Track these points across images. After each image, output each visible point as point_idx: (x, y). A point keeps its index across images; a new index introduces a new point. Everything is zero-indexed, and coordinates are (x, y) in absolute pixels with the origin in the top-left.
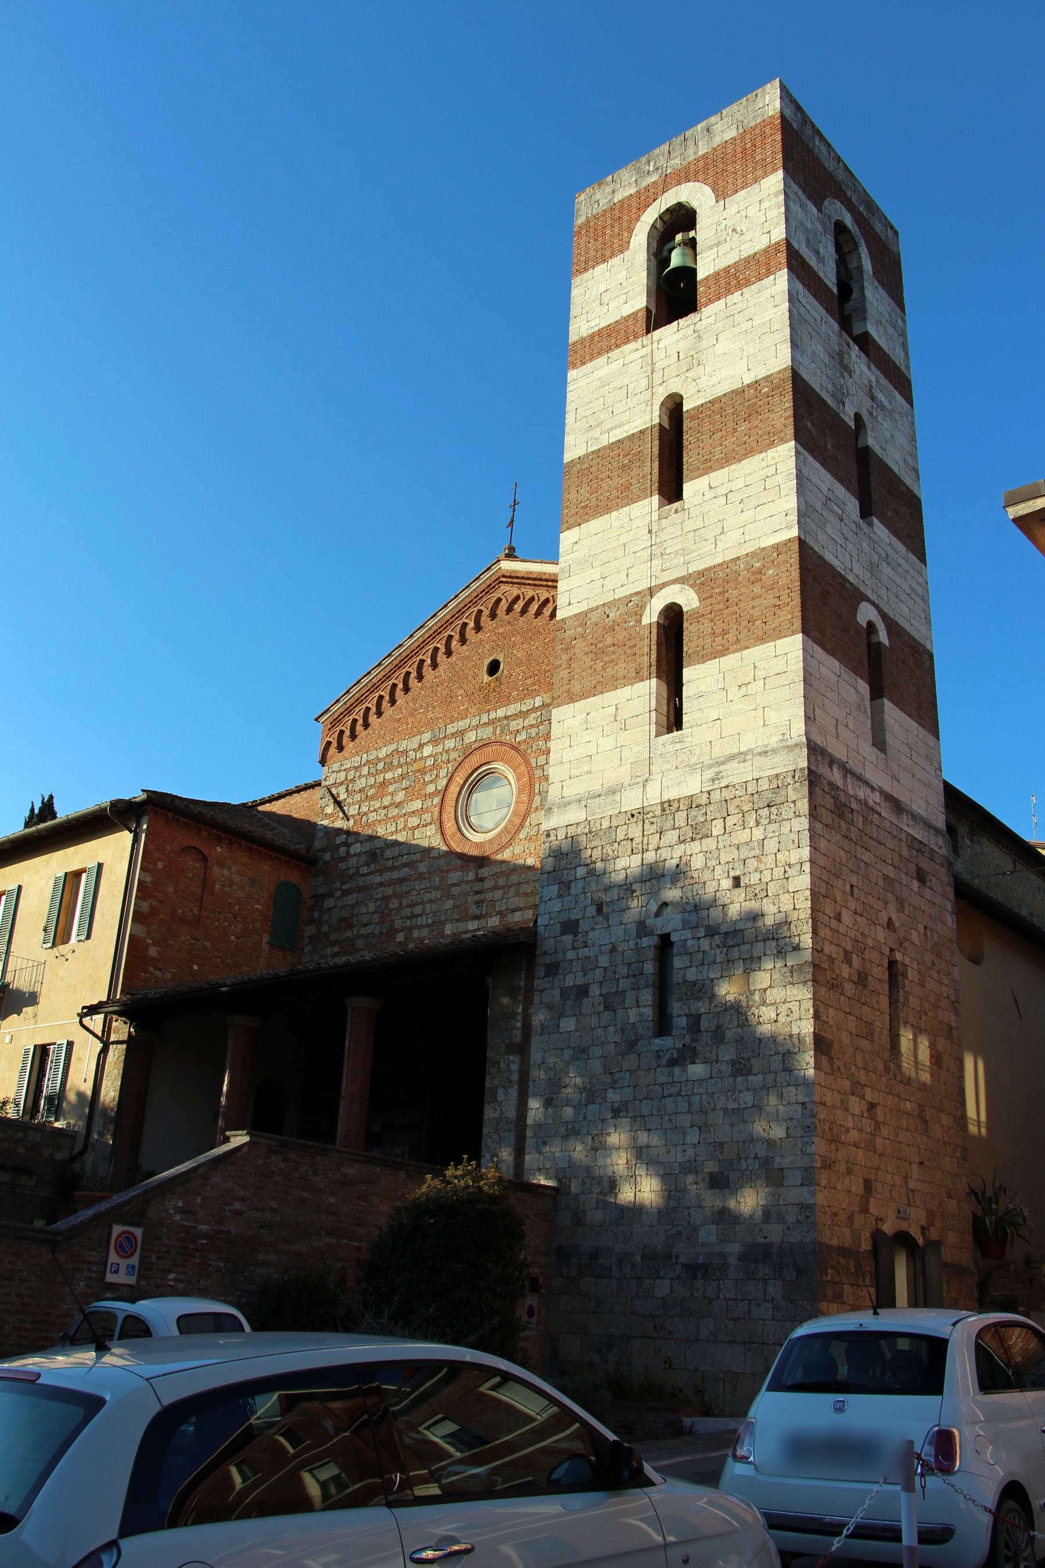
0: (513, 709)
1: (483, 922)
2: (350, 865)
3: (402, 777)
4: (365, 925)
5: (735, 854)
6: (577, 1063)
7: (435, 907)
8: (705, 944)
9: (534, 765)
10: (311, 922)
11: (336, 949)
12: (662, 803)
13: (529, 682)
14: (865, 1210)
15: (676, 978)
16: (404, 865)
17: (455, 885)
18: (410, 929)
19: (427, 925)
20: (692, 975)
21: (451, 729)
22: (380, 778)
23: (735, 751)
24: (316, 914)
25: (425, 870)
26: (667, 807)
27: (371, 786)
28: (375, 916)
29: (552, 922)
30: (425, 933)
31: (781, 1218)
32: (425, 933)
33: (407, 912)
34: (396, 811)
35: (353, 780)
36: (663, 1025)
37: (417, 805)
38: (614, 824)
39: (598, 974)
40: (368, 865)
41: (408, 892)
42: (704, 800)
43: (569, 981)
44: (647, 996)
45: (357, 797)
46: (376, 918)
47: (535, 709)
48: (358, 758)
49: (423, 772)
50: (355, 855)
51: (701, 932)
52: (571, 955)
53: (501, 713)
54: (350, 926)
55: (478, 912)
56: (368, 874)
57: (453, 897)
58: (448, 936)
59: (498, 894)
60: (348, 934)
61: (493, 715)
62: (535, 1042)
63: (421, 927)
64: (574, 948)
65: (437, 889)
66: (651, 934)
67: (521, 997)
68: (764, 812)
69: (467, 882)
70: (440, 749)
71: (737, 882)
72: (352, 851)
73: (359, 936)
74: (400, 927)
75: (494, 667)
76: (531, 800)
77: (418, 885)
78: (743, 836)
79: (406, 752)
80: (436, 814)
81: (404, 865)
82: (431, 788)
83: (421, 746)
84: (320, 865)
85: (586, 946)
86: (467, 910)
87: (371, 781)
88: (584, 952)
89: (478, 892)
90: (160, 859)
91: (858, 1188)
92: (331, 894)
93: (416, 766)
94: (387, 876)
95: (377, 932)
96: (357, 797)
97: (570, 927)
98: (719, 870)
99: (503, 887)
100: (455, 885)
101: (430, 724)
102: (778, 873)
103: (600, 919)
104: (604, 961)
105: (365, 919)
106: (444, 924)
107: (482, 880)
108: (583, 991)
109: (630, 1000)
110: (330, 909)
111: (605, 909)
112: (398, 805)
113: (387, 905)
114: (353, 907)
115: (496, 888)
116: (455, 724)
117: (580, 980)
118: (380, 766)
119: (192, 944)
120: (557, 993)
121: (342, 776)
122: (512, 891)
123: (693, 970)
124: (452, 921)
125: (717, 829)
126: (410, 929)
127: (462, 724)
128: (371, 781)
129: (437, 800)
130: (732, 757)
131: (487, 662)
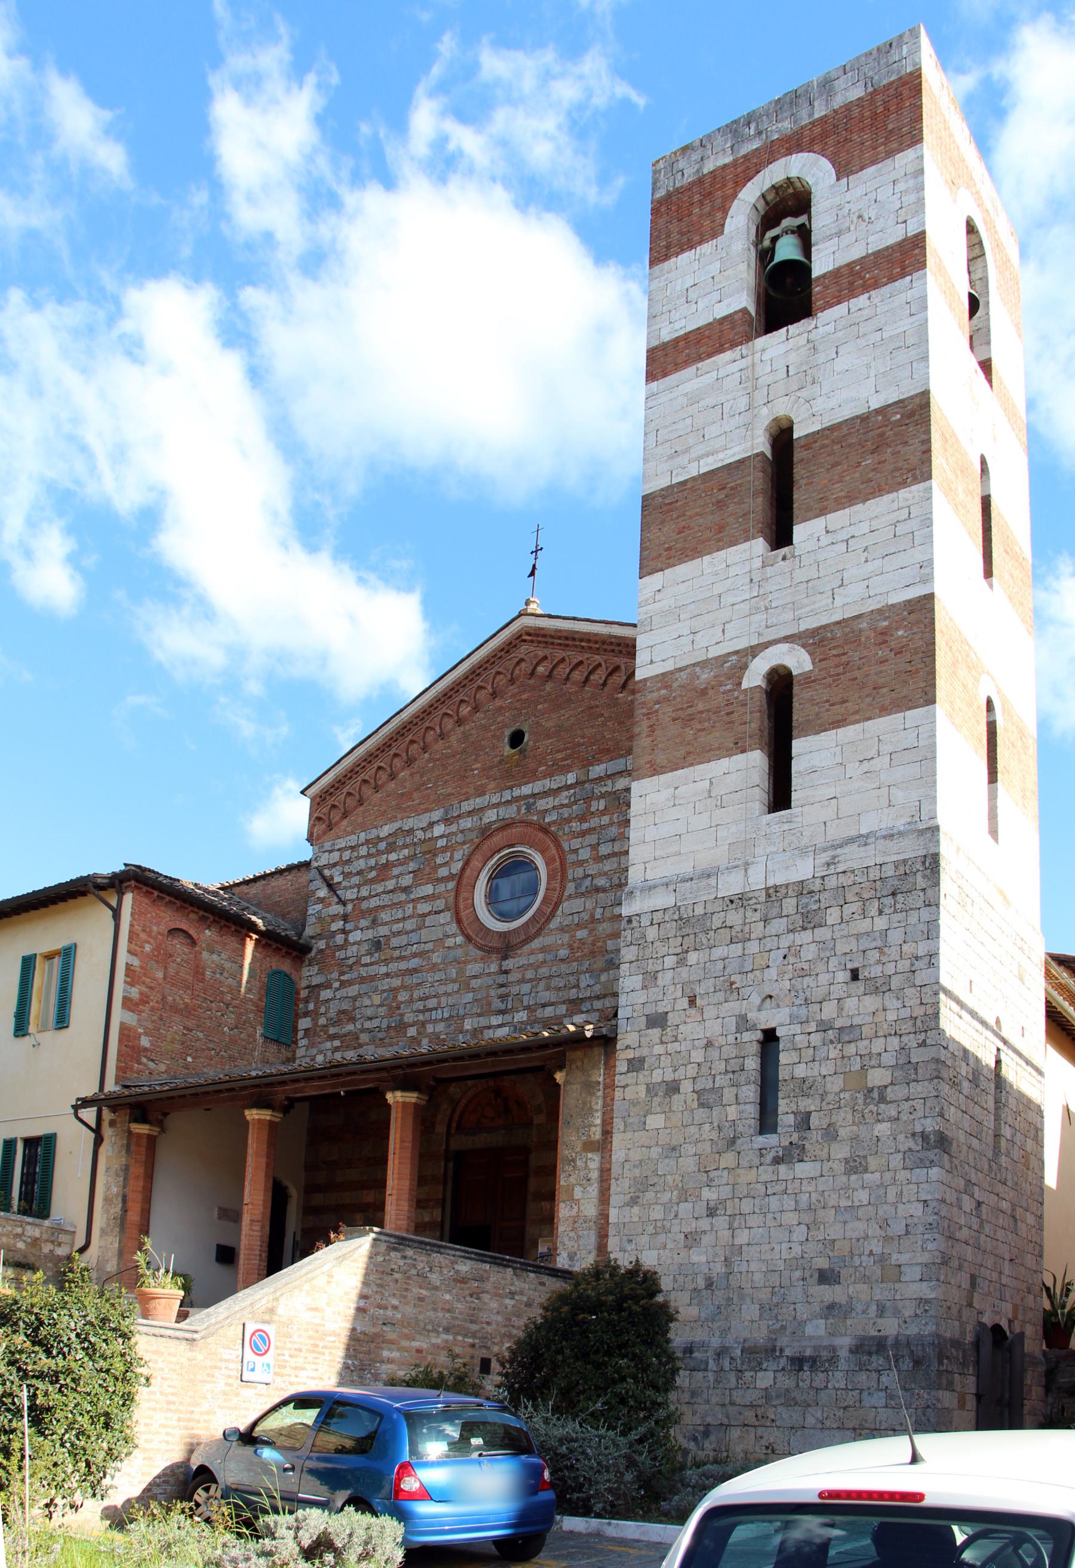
0: (538, 786)
1: (508, 1018)
4: (370, 1019)
6: (667, 1161)
8: (816, 1039)
9: (567, 849)
12: (767, 889)
13: (560, 756)
14: (970, 1305)
15: (783, 1074)
16: (415, 955)
17: (475, 977)
18: (423, 1024)
19: (442, 1020)
20: (800, 1071)
21: (466, 806)
22: (383, 859)
23: (853, 833)
24: (311, 1006)
25: (439, 961)
27: (372, 868)
28: (380, 1009)
29: (635, 1015)
30: (440, 1027)
31: (897, 1313)
32: (440, 1027)
33: (420, 1005)
34: (403, 897)
35: (349, 861)
36: (767, 1122)
37: (428, 889)
39: (692, 1070)
41: (419, 984)
43: (657, 1077)
44: (751, 1093)
45: (356, 880)
46: (382, 1011)
47: (568, 787)
48: (354, 837)
49: (434, 852)
50: (354, 943)
51: (812, 1027)
52: (659, 1049)
53: (526, 790)
54: (353, 1020)
55: (503, 1007)
56: (372, 964)
57: (474, 990)
58: (467, 1031)
59: (526, 988)
60: (350, 1027)
61: (517, 792)
63: (436, 1021)
64: (662, 1042)
65: (454, 981)
66: (753, 1028)
67: (600, 1093)
69: (489, 974)
70: (454, 828)
74: (411, 1021)
75: (516, 739)
76: (563, 888)
77: (430, 977)
79: (411, 831)
80: (451, 899)
81: (415, 955)
82: (443, 872)
83: (431, 825)
84: (313, 954)
85: (676, 1041)
86: (489, 1004)
87: (372, 862)
88: (673, 1047)
89: (502, 986)
90: (148, 942)
91: (966, 1284)
92: (327, 985)
93: (425, 847)
94: (393, 967)
95: (384, 1026)
96: (356, 880)
97: (657, 1021)
99: (530, 981)
100: (475, 977)
101: (441, 801)
103: (693, 1011)
104: (698, 1056)
105: (369, 1012)
106: (463, 1018)
107: (506, 972)
108: (673, 1088)
109: (728, 1095)
110: (328, 1001)
111: (698, 1002)
112: (406, 890)
114: (354, 999)
115: (523, 981)
116: (471, 802)
117: (669, 1076)
118: (382, 846)
119: (184, 1034)
120: (642, 1089)
121: (335, 856)
122: (542, 984)
123: (803, 1066)
126: (423, 1024)
127: (479, 802)
128: (372, 862)
129: (451, 885)
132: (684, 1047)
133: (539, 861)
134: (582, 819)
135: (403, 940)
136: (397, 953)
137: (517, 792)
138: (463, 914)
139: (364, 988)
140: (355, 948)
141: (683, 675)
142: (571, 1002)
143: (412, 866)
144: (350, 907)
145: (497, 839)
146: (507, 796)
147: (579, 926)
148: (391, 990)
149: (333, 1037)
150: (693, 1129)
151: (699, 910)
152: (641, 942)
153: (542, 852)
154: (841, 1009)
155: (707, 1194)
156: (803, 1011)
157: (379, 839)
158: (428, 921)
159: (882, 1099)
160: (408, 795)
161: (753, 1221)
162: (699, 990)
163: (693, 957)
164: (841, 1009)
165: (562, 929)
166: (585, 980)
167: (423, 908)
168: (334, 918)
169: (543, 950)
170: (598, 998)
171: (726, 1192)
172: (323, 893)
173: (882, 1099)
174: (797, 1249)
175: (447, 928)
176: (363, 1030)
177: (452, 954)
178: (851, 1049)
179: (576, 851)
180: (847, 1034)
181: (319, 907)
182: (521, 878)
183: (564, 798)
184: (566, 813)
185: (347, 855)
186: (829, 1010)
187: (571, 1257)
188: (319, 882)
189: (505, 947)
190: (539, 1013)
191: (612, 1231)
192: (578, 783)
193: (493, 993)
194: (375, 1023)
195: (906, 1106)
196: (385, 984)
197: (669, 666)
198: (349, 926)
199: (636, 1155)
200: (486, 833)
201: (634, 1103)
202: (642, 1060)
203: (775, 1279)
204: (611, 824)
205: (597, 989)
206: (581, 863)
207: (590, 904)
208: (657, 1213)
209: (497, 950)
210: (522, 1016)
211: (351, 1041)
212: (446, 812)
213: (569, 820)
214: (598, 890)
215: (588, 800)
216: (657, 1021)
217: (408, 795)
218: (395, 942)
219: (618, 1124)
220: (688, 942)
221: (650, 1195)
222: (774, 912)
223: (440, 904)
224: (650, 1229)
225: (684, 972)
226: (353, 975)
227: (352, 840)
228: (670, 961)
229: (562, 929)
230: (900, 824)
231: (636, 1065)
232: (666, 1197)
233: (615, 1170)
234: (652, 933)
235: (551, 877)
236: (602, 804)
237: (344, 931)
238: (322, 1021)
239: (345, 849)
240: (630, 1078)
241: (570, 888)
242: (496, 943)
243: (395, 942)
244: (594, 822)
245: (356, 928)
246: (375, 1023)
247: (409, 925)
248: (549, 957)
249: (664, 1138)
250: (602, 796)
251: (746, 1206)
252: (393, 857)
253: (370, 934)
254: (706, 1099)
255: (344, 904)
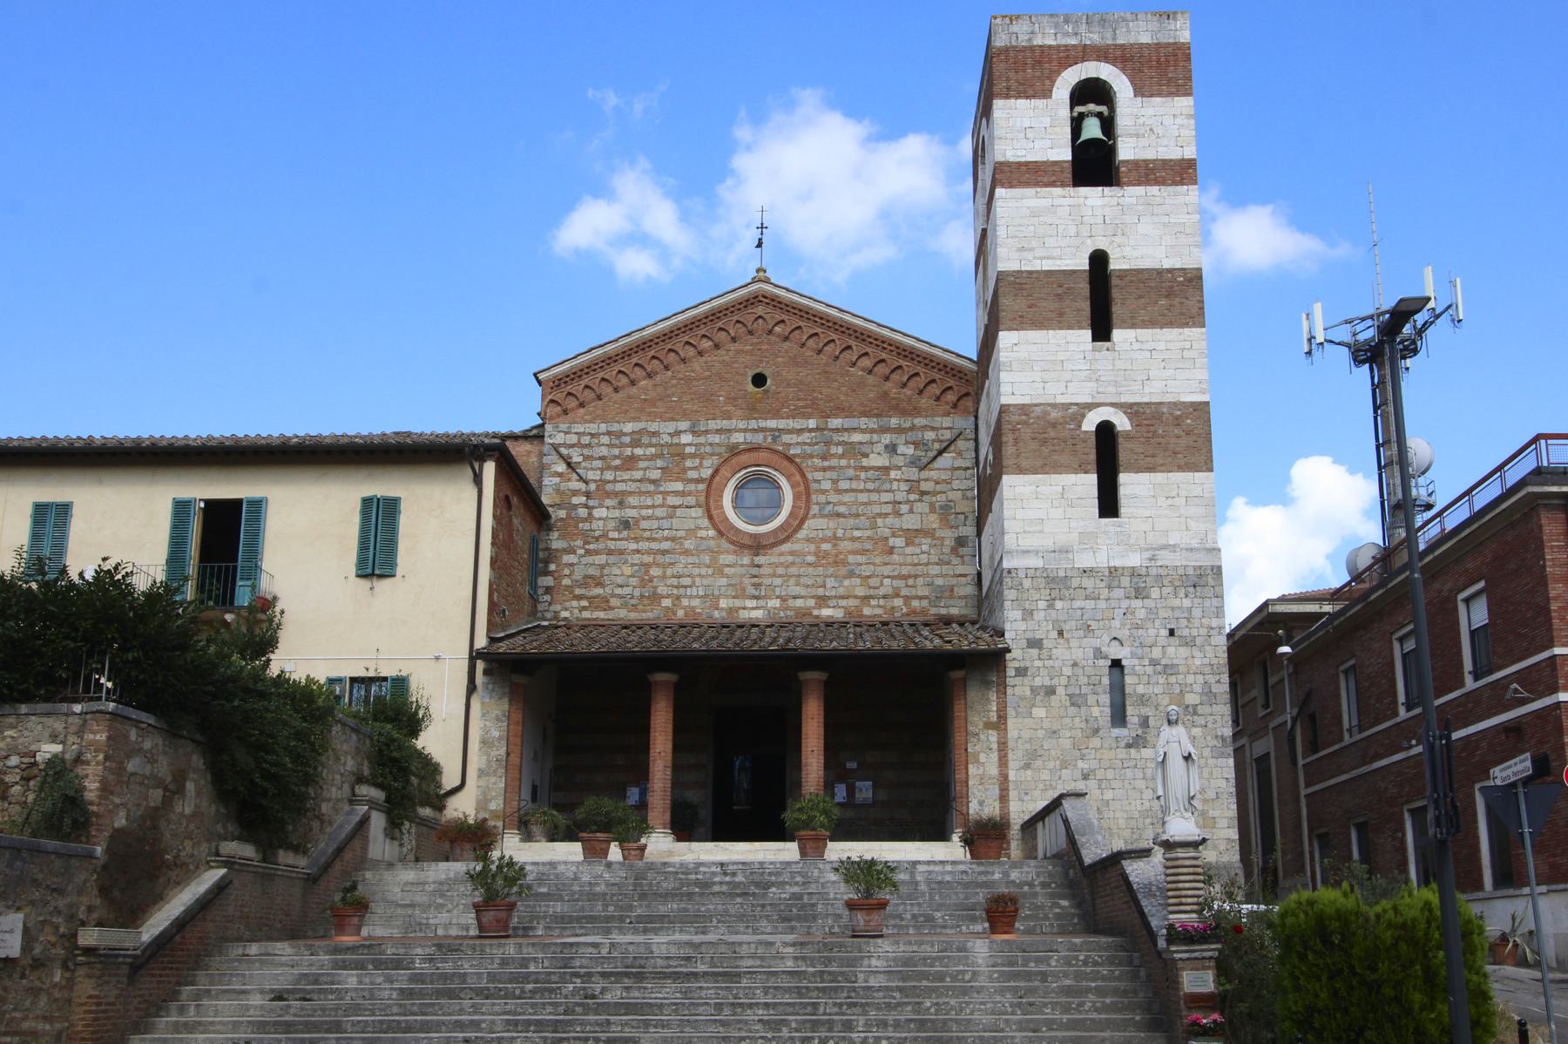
0: (782, 424)
1: (761, 603)
2: (594, 526)
3: (653, 458)
5: (1170, 613)
7: (705, 582)
8: (1149, 670)
10: (547, 573)
11: (584, 603)
15: (1128, 690)
16: (667, 539)
18: (678, 598)
19: (697, 596)
20: (1141, 689)
22: (628, 451)
26: (1113, 571)
27: (616, 457)
30: (695, 603)
33: (675, 581)
34: (652, 488)
35: (589, 446)
37: (679, 486)
38: (1069, 574)
40: (616, 529)
42: (1143, 572)
43: (1038, 682)
44: (1105, 699)
47: (810, 431)
49: (683, 457)
52: (1037, 663)
53: (772, 424)
54: (600, 584)
59: (778, 581)
61: (762, 424)
62: (1010, 722)
63: (691, 597)
66: (1106, 657)
68: (1191, 589)
70: (702, 440)
71: (1172, 633)
72: (596, 513)
73: (613, 595)
75: (759, 380)
76: (808, 509)
78: (1177, 602)
80: (702, 499)
81: (667, 539)
82: (693, 474)
83: (678, 433)
86: (744, 590)
87: (616, 452)
92: (572, 551)
94: (644, 545)
95: (637, 593)
96: (598, 464)
97: (1035, 643)
98: (1157, 622)
101: (685, 415)
102: (1203, 631)
104: (1067, 671)
105: (619, 580)
106: (718, 598)
107: (759, 566)
108: (1051, 691)
109: (1091, 699)
110: (572, 565)
112: (653, 482)
113: (647, 572)
114: (602, 567)
115: (774, 575)
117: (1047, 682)
118: (627, 440)
121: (573, 439)
122: (792, 581)
124: (726, 597)
125: (1155, 593)
126: (678, 598)
127: (725, 424)
128: (616, 452)
129: (702, 487)
130: (1164, 547)
131: (750, 374)
132: (1057, 664)
133: (783, 482)
134: (824, 458)
135: (655, 524)
136: (647, 534)
137: (762, 424)
138: (714, 512)
139: (612, 559)
140: (601, 523)
141: (1038, 409)
142: (819, 598)
143: (659, 463)
144: (593, 487)
145: (745, 458)
146: (753, 424)
147: (824, 540)
148: (643, 564)
149: (579, 598)
150: (1067, 720)
151: (1062, 574)
152: (1019, 587)
153: (788, 478)
154: (1164, 653)
155: (1081, 764)
156: (1139, 651)
157: (621, 434)
158: (679, 512)
159: (1195, 713)
160: (652, 403)
161: (1114, 784)
162: (1066, 627)
163: (1059, 604)
164: (1164, 653)
165: (808, 540)
166: (830, 582)
167: (672, 500)
168: (575, 493)
169: (792, 553)
170: (842, 598)
171: (1094, 764)
172: (561, 467)
173: (1195, 713)
174: (1147, 804)
175: (699, 522)
176: (613, 595)
177: (704, 545)
178: (1173, 679)
179: (818, 482)
180: (1169, 669)
181: (557, 480)
182: (763, 494)
183: (806, 437)
184: (809, 450)
185: (586, 440)
186: (1156, 653)
187: (981, 803)
188: (554, 457)
189: (757, 545)
190: (791, 603)
191: (1011, 786)
192: (817, 429)
193: (746, 581)
194: (627, 591)
195: (1210, 719)
196: (637, 558)
197: (1027, 400)
198: (591, 503)
199: (1026, 734)
200: (734, 451)
201: (1022, 698)
202: (1026, 669)
203: (1133, 823)
204: (849, 467)
205: (841, 591)
206: (824, 492)
207: (832, 525)
208: (1045, 775)
209: (750, 547)
210: (774, 603)
211: (604, 602)
212: (694, 425)
213: (811, 456)
214: (838, 515)
215: (828, 443)
216: (1035, 643)
217: (652, 403)
218: (644, 524)
219: (1010, 712)
220: (1055, 593)
221: (1039, 763)
222: (1115, 583)
223: (691, 500)
224: (1041, 786)
225: (1053, 613)
226: (601, 546)
227: (593, 428)
228: (1042, 605)
229: (808, 540)
230: (1195, 544)
231: (1022, 672)
232: (1051, 765)
233: (1011, 744)
234: (1027, 583)
235: (796, 497)
236: (840, 450)
237: (586, 506)
238: (566, 582)
239: (584, 434)
240: (1018, 680)
241: (815, 509)
242: (747, 541)
243: (644, 524)
244: (834, 462)
245: (601, 506)
246: (627, 591)
247: (660, 512)
248: (798, 560)
249: (1046, 724)
250: (838, 444)
251: (1110, 774)
252: (639, 451)
253: (617, 513)
254: (1076, 701)
255: (586, 482)
